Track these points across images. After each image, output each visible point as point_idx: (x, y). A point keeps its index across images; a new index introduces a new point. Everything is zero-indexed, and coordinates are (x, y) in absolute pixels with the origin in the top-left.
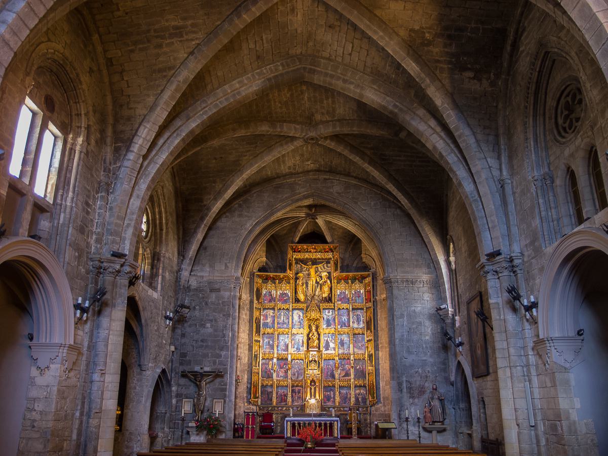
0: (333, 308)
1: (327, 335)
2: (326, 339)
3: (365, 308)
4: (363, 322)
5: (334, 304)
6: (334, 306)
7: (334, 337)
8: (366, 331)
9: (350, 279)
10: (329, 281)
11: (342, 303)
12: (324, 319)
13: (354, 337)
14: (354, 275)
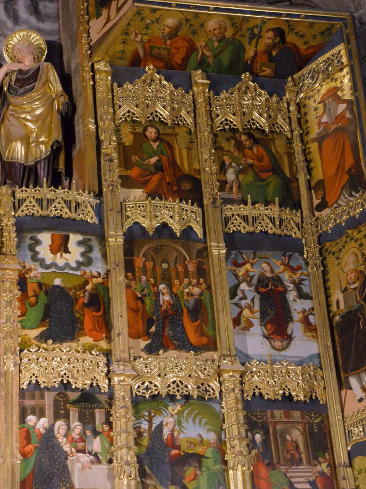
0: (91, 218)
1: (49, 398)
2: (42, 424)
3: (312, 240)
4: (309, 327)
5: (99, 195)
6: (99, 210)
7: (99, 416)
8: (333, 383)
9: (202, 64)
10: (53, 76)
11: (152, 195)
12: (22, 282)
13: (251, 425)
14: (237, 24)
